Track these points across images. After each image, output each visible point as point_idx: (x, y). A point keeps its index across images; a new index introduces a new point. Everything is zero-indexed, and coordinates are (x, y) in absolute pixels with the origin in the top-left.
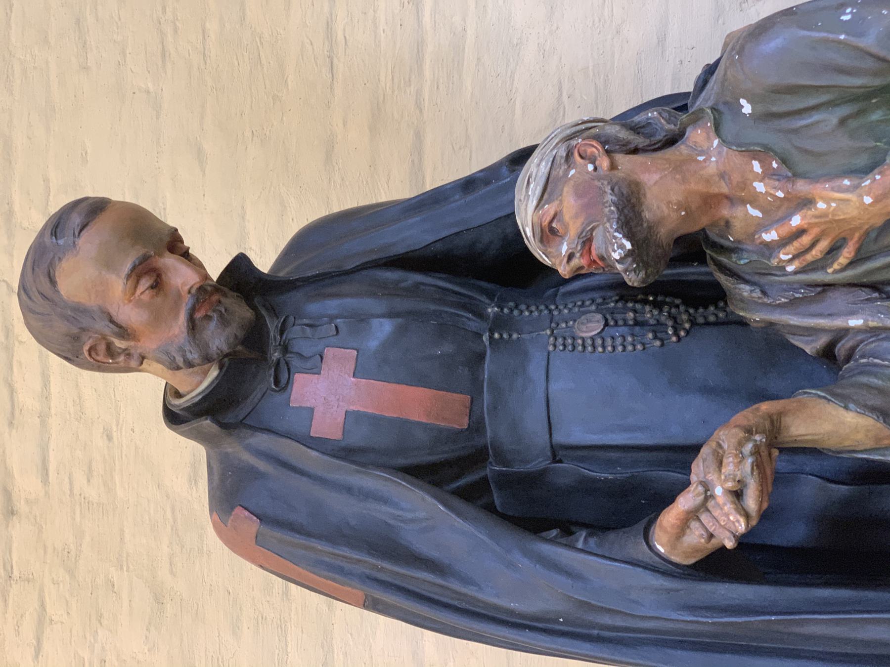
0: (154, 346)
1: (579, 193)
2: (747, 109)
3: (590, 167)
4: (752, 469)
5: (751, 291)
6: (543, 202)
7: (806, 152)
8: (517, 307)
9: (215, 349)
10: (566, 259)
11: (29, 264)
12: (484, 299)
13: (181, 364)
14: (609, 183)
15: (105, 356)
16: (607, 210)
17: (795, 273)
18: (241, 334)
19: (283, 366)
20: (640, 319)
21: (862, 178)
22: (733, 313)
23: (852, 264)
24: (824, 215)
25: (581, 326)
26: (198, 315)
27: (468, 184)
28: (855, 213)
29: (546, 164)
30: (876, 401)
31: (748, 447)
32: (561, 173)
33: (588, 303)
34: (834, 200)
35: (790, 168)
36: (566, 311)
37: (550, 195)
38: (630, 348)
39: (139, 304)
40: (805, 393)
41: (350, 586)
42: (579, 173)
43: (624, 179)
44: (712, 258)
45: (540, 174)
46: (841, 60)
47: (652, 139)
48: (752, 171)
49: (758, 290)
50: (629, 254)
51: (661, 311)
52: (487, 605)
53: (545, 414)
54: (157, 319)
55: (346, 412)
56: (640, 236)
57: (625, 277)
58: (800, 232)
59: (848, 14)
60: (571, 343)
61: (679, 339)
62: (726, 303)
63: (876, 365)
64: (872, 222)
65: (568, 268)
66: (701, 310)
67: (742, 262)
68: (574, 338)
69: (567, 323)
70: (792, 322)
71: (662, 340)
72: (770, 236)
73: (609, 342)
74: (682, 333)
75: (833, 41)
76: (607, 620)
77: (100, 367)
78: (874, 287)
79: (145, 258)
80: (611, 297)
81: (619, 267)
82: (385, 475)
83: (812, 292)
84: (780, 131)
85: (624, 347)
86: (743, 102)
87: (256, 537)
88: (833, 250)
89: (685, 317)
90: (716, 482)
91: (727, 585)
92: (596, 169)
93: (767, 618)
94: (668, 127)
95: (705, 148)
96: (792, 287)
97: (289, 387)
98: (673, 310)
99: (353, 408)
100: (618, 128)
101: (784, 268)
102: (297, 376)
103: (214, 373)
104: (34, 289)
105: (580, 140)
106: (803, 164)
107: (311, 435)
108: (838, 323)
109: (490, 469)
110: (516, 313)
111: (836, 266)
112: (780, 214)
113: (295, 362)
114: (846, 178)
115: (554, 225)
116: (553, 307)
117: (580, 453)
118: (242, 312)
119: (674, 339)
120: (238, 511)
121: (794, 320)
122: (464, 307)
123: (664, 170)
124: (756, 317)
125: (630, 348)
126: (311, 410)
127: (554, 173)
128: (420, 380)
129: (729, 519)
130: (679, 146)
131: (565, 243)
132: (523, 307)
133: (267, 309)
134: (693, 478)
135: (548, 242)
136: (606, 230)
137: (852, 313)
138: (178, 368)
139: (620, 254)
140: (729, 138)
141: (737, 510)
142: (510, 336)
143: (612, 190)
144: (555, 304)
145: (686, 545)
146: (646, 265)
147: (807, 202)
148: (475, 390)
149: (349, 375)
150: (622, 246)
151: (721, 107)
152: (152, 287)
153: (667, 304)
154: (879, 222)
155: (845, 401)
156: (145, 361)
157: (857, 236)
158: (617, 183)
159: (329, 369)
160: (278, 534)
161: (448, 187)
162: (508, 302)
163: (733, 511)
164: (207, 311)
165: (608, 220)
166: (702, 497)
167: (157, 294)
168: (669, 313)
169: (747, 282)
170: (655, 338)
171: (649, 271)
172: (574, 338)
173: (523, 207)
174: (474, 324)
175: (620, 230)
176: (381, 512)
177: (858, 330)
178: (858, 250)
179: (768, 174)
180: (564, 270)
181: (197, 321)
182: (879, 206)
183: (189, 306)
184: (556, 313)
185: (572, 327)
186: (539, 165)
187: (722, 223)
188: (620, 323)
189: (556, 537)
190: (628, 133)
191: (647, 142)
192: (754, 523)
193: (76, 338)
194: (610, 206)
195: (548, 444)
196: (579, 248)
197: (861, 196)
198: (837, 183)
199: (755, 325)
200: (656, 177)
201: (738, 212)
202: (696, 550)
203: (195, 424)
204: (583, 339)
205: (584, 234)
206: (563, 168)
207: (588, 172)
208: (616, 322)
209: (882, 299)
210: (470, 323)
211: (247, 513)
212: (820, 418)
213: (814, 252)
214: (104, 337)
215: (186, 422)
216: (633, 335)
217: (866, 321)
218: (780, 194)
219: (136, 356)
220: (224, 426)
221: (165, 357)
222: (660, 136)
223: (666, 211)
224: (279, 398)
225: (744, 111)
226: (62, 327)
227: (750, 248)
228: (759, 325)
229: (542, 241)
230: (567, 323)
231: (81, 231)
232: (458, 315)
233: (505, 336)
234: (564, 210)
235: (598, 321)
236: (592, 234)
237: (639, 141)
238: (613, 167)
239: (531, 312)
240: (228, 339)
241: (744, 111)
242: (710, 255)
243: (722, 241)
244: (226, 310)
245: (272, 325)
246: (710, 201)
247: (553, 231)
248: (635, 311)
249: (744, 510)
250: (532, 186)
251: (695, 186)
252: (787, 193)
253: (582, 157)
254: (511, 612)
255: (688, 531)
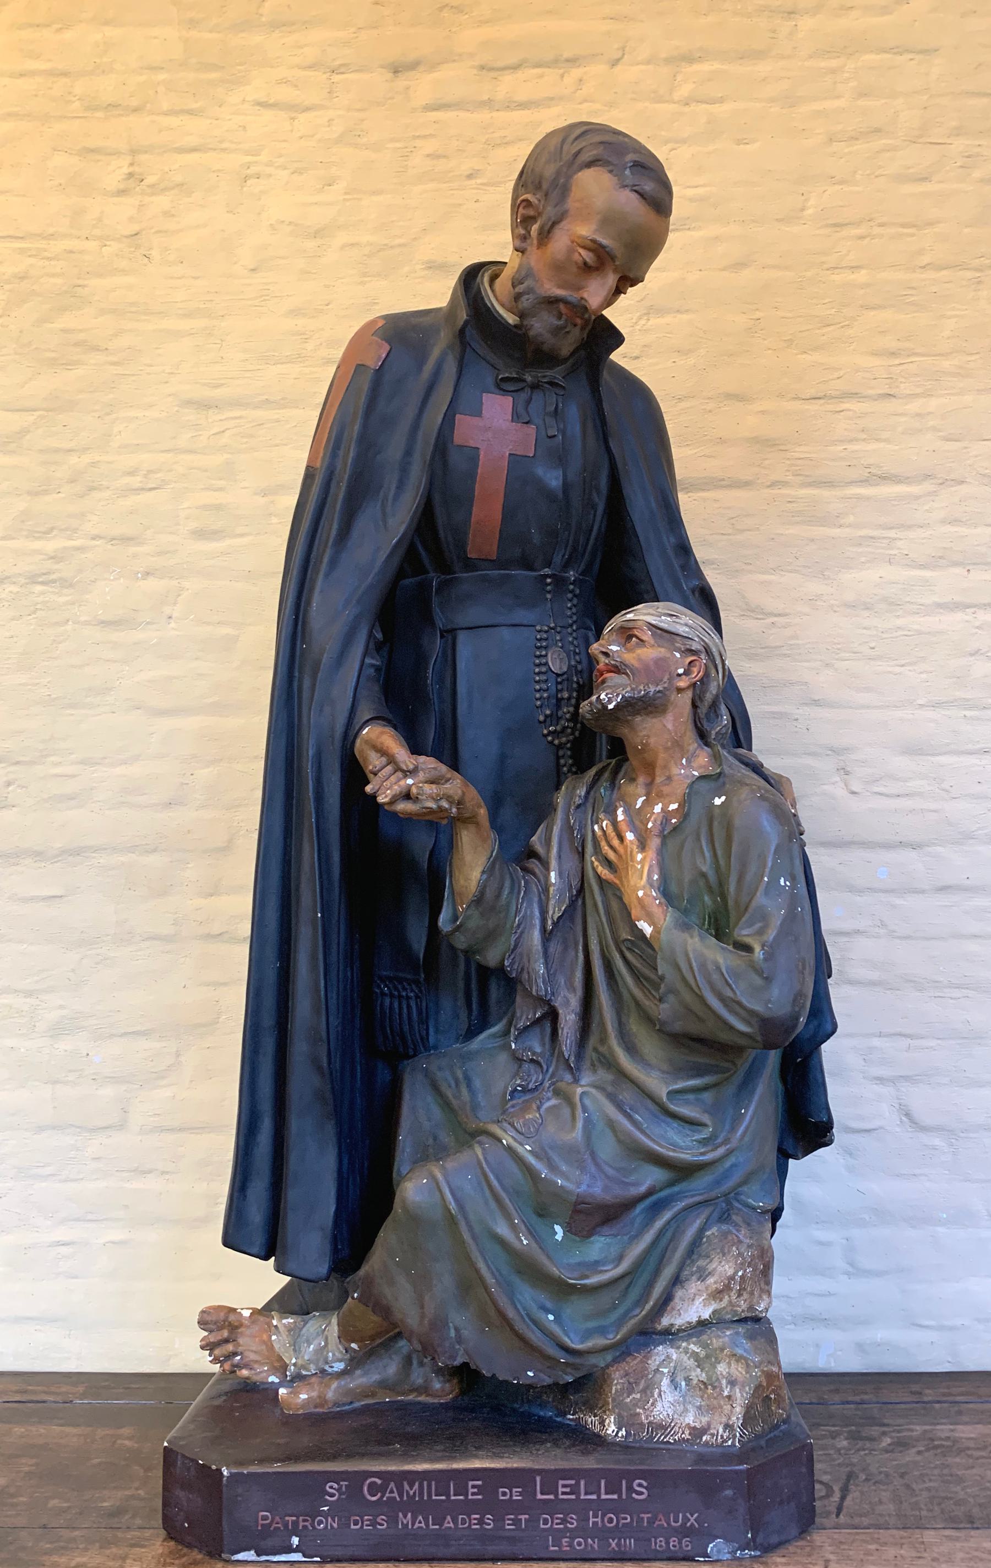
0: (533, 264)
1: (659, 662)
2: (718, 801)
3: (681, 671)
4: (428, 808)
5: (580, 796)
6: (654, 629)
7: (682, 846)
8: (575, 596)
9: (532, 323)
10: (604, 650)
11: (607, 138)
12: (582, 566)
13: (517, 290)
14: (665, 688)
15: (523, 215)
16: (642, 687)
17: (593, 831)
18: (545, 347)
19: (521, 385)
20: (563, 703)
21: (659, 889)
22: (567, 778)
23: (598, 877)
24: (633, 858)
25: (557, 654)
26: (562, 306)
27: (684, 549)
28: (632, 883)
29: (687, 632)
30: (489, 894)
31: (445, 804)
32: (678, 645)
33: (577, 658)
34: (643, 867)
35: (669, 833)
36: (570, 639)
37: (661, 636)
38: (538, 695)
39: (571, 251)
40: (496, 841)
41: (325, 454)
42: (677, 661)
43: (668, 701)
44: (609, 764)
45: (678, 626)
46: (749, 877)
47: (705, 720)
48: (671, 802)
49: (581, 801)
50: (605, 707)
51: (568, 720)
52: (314, 581)
53: (481, 624)
54: (558, 268)
55: (478, 449)
56: (620, 714)
57: (586, 702)
58: (621, 838)
59: (785, 883)
60: (542, 646)
61: (545, 736)
62: (576, 773)
63: (519, 893)
64: (625, 894)
65: (596, 652)
66: (569, 753)
67: (602, 791)
68: (546, 648)
69: (561, 640)
70: (555, 827)
71: (545, 721)
72: (620, 816)
73: (544, 678)
74: (550, 738)
75: (764, 872)
76: (307, 683)
77: (515, 207)
78: (581, 890)
79: (613, 258)
80: (582, 678)
81: (594, 698)
82: (422, 488)
83: (578, 844)
84: (699, 828)
85: (539, 691)
86: (723, 798)
87: (363, 365)
88: (609, 863)
89: (564, 740)
90: (416, 780)
91: (338, 783)
92: (679, 675)
93: (314, 815)
94: (713, 732)
95: (692, 764)
96: (582, 827)
97: (502, 392)
98: (569, 731)
99: (482, 453)
100: (714, 692)
101: (597, 823)
102: (511, 399)
103: (511, 319)
104: (584, 144)
105: (704, 661)
106: (672, 844)
107: (457, 416)
108: (553, 863)
109: (433, 577)
110: (570, 596)
111: (596, 863)
112: (637, 823)
113: (524, 396)
114: (659, 877)
115: (634, 639)
116: (574, 627)
117: (449, 652)
118: (566, 347)
119: (545, 732)
120: (387, 347)
121: (556, 830)
122: (575, 549)
123: (676, 734)
124: (560, 799)
125: (538, 695)
126: (479, 414)
127: (678, 638)
128: (509, 513)
129: (388, 789)
130: (697, 742)
131: (619, 648)
132: (575, 601)
133: (574, 365)
134: (422, 759)
135: (622, 633)
136: (626, 686)
137: (560, 874)
138: (514, 286)
139: (604, 699)
140: (695, 786)
141: (394, 796)
142: (549, 592)
143: (659, 692)
144: (577, 629)
145: (369, 752)
146: (597, 719)
147: (643, 846)
148: (499, 563)
149: (511, 450)
150: (610, 701)
151: (721, 780)
152: (585, 263)
153: (575, 725)
154: (626, 900)
155: (489, 871)
156: (520, 254)
157: (617, 882)
158: (665, 695)
159: (516, 430)
160: (366, 387)
161: (683, 532)
162: (580, 589)
163: (394, 793)
164: (566, 315)
165: (633, 689)
166: (405, 768)
167: (579, 268)
168: (568, 727)
169: (588, 793)
170: (546, 716)
171: (593, 722)
172: (546, 648)
173: (651, 611)
174: (558, 559)
175: (624, 699)
176: (391, 481)
177: (547, 877)
178: (606, 881)
179: (666, 815)
180: (595, 648)
181: (555, 306)
182: (635, 901)
183: (570, 299)
184: (569, 630)
185: (556, 645)
186: (686, 625)
187: (634, 776)
188: (560, 687)
189: (375, 637)
190: (710, 700)
191: (702, 716)
192: (386, 807)
193: (538, 187)
194: (645, 690)
195: (457, 627)
196: (612, 662)
197: (643, 888)
198: (656, 869)
199: (555, 797)
200: (670, 726)
201: (641, 789)
202: (365, 759)
203: (462, 303)
204: (546, 656)
205: (624, 667)
206: (682, 646)
207: (677, 669)
208: (560, 683)
209: (571, 896)
210: (560, 556)
211: (384, 356)
212: (475, 853)
213: (606, 848)
214: (540, 214)
215: (466, 295)
216: (549, 697)
217: (554, 885)
218: (650, 825)
219: (524, 245)
220: (462, 332)
221: (523, 273)
222: (706, 725)
223: (641, 734)
224: (490, 381)
225: (717, 798)
226: (549, 171)
227: (614, 796)
228: (555, 800)
229: (622, 627)
230: (561, 640)
231: (636, 191)
232: (566, 547)
233: (549, 588)
234: (645, 649)
235: (561, 668)
236: (623, 673)
237: (703, 710)
238: (680, 690)
239: (570, 609)
240: (541, 335)
241: (717, 798)
242: (610, 763)
243: (621, 774)
244: (568, 332)
245: (556, 374)
246: (650, 768)
247: (630, 637)
248: (569, 699)
249: (396, 801)
250: (669, 619)
251: (662, 756)
252: (651, 830)
253: (690, 663)
254: (309, 603)
255: (379, 755)
